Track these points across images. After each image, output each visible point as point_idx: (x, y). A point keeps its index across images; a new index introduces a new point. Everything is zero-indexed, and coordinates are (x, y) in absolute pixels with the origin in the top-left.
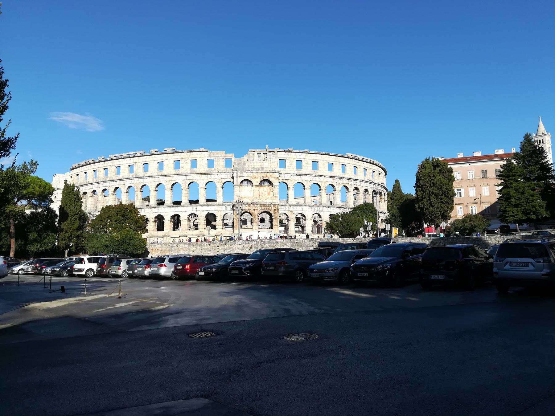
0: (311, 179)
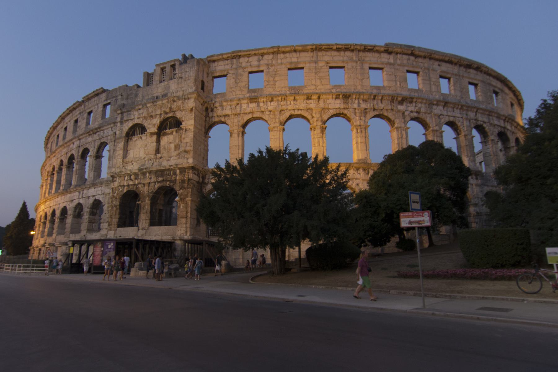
0: (284, 108)
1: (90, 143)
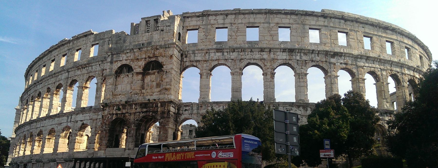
0: (243, 57)
1: (79, 76)
